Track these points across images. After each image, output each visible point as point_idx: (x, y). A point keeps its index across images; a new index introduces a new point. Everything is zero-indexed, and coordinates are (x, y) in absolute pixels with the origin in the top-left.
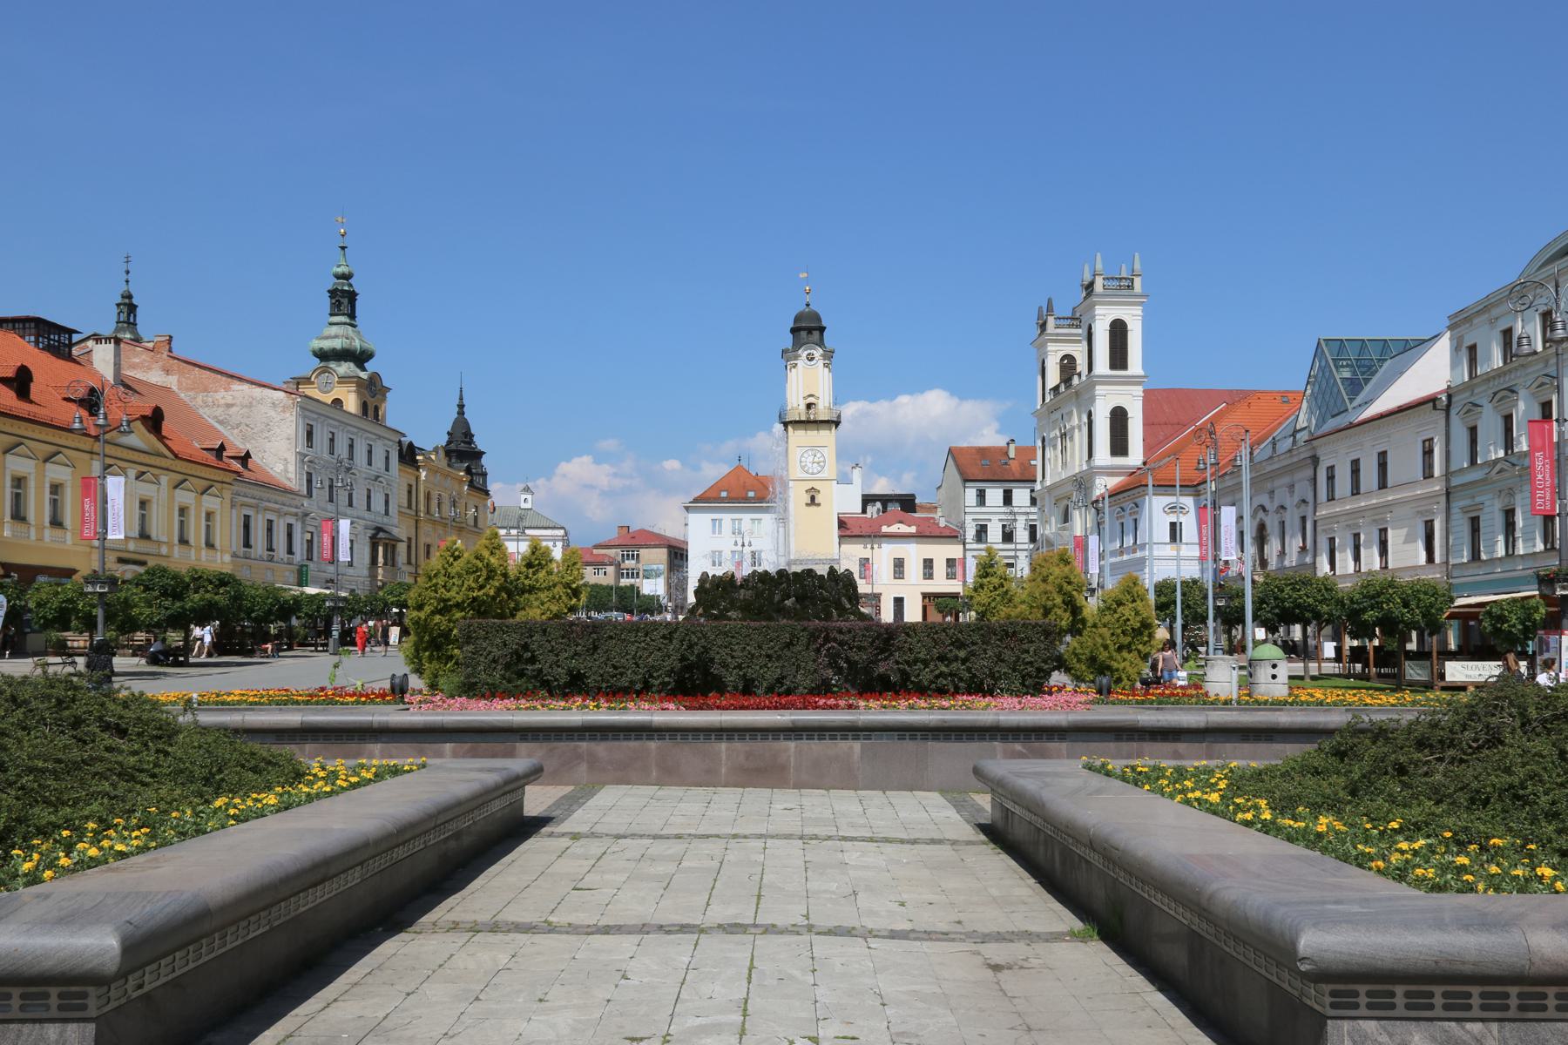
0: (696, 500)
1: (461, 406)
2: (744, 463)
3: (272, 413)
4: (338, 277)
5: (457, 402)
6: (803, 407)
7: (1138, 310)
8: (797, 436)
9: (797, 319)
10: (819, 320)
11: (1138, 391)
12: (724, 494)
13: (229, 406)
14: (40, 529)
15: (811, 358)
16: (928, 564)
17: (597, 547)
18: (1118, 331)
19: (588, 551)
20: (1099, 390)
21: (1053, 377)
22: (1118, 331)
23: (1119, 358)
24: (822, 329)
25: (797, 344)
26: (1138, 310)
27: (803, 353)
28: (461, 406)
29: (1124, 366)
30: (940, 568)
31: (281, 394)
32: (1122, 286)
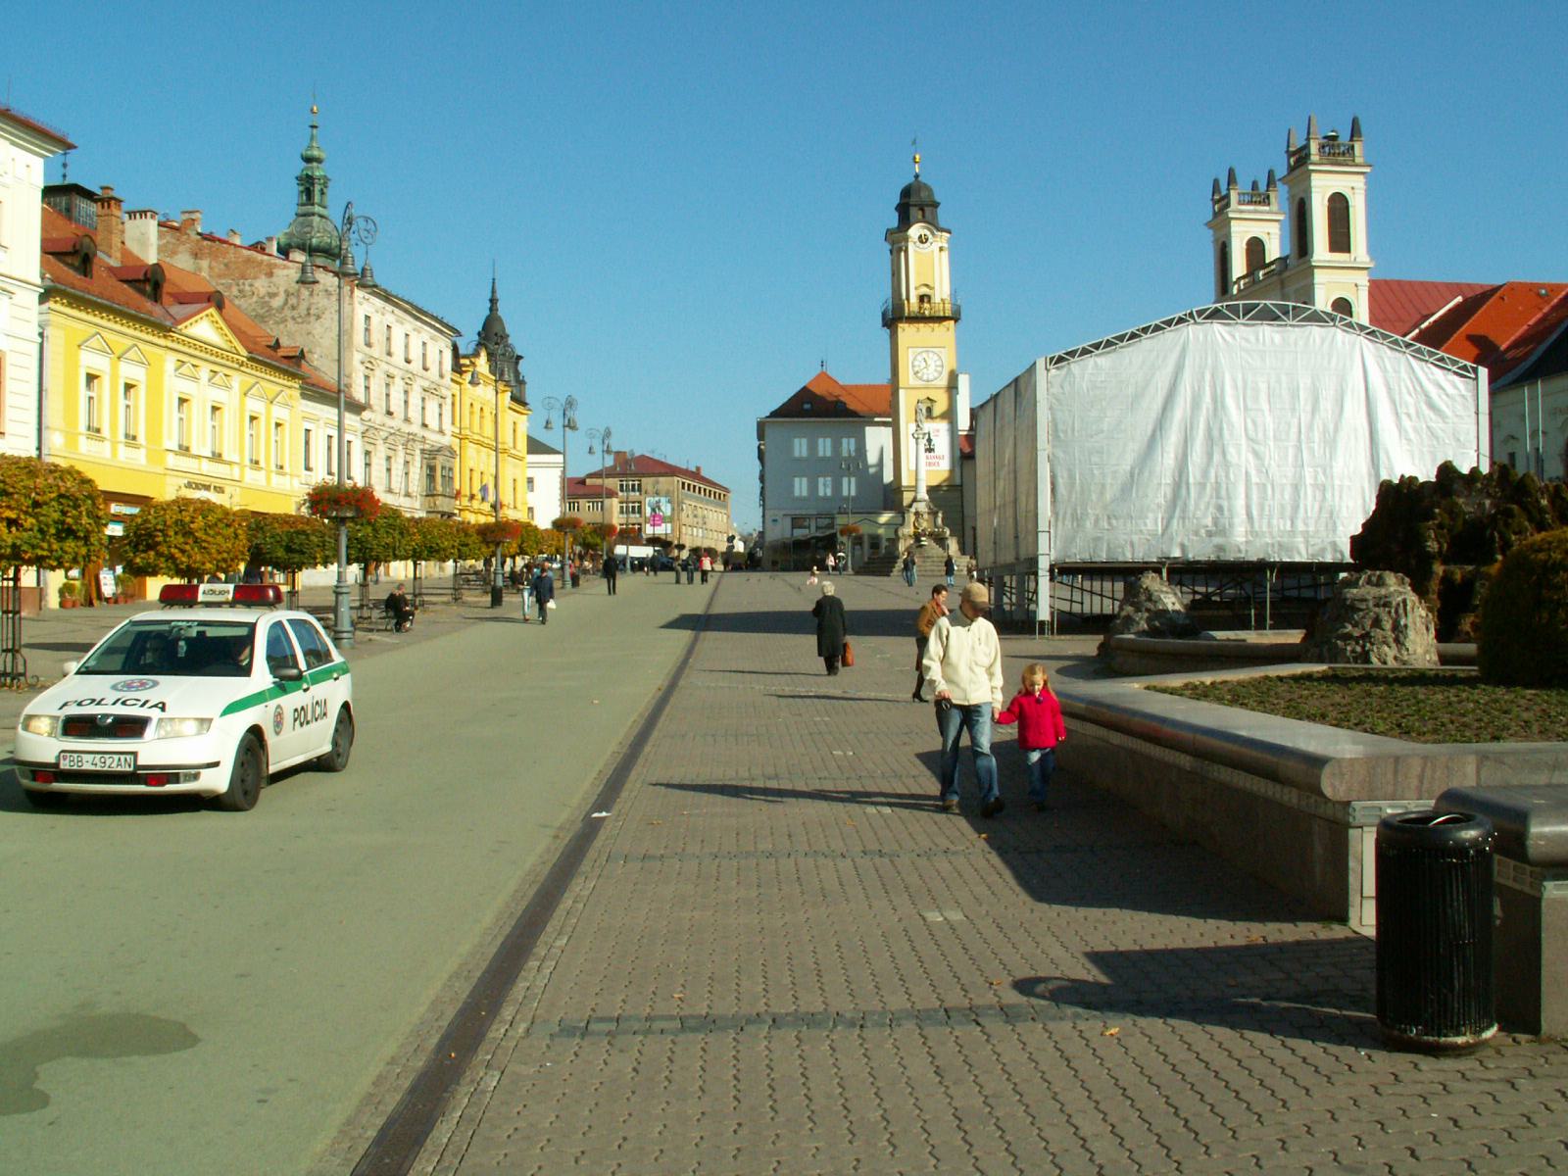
0: (775, 414)
1: (493, 301)
4: (308, 160)
5: (489, 296)
6: (914, 300)
7: (1359, 182)
8: (906, 332)
9: (906, 193)
11: (1363, 279)
12: (807, 406)
14: (114, 443)
15: (922, 240)
17: (591, 476)
18: (1339, 206)
19: (582, 482)
20: (1319, 277)
21: (1239, 267)
22: (1339, 206)
23: (1340, 240)
24: (935, 205)
25: (905, 222)
27: (915, 231)
28: (493, 301)
29: (1346, 249)
32: (1337, 151)
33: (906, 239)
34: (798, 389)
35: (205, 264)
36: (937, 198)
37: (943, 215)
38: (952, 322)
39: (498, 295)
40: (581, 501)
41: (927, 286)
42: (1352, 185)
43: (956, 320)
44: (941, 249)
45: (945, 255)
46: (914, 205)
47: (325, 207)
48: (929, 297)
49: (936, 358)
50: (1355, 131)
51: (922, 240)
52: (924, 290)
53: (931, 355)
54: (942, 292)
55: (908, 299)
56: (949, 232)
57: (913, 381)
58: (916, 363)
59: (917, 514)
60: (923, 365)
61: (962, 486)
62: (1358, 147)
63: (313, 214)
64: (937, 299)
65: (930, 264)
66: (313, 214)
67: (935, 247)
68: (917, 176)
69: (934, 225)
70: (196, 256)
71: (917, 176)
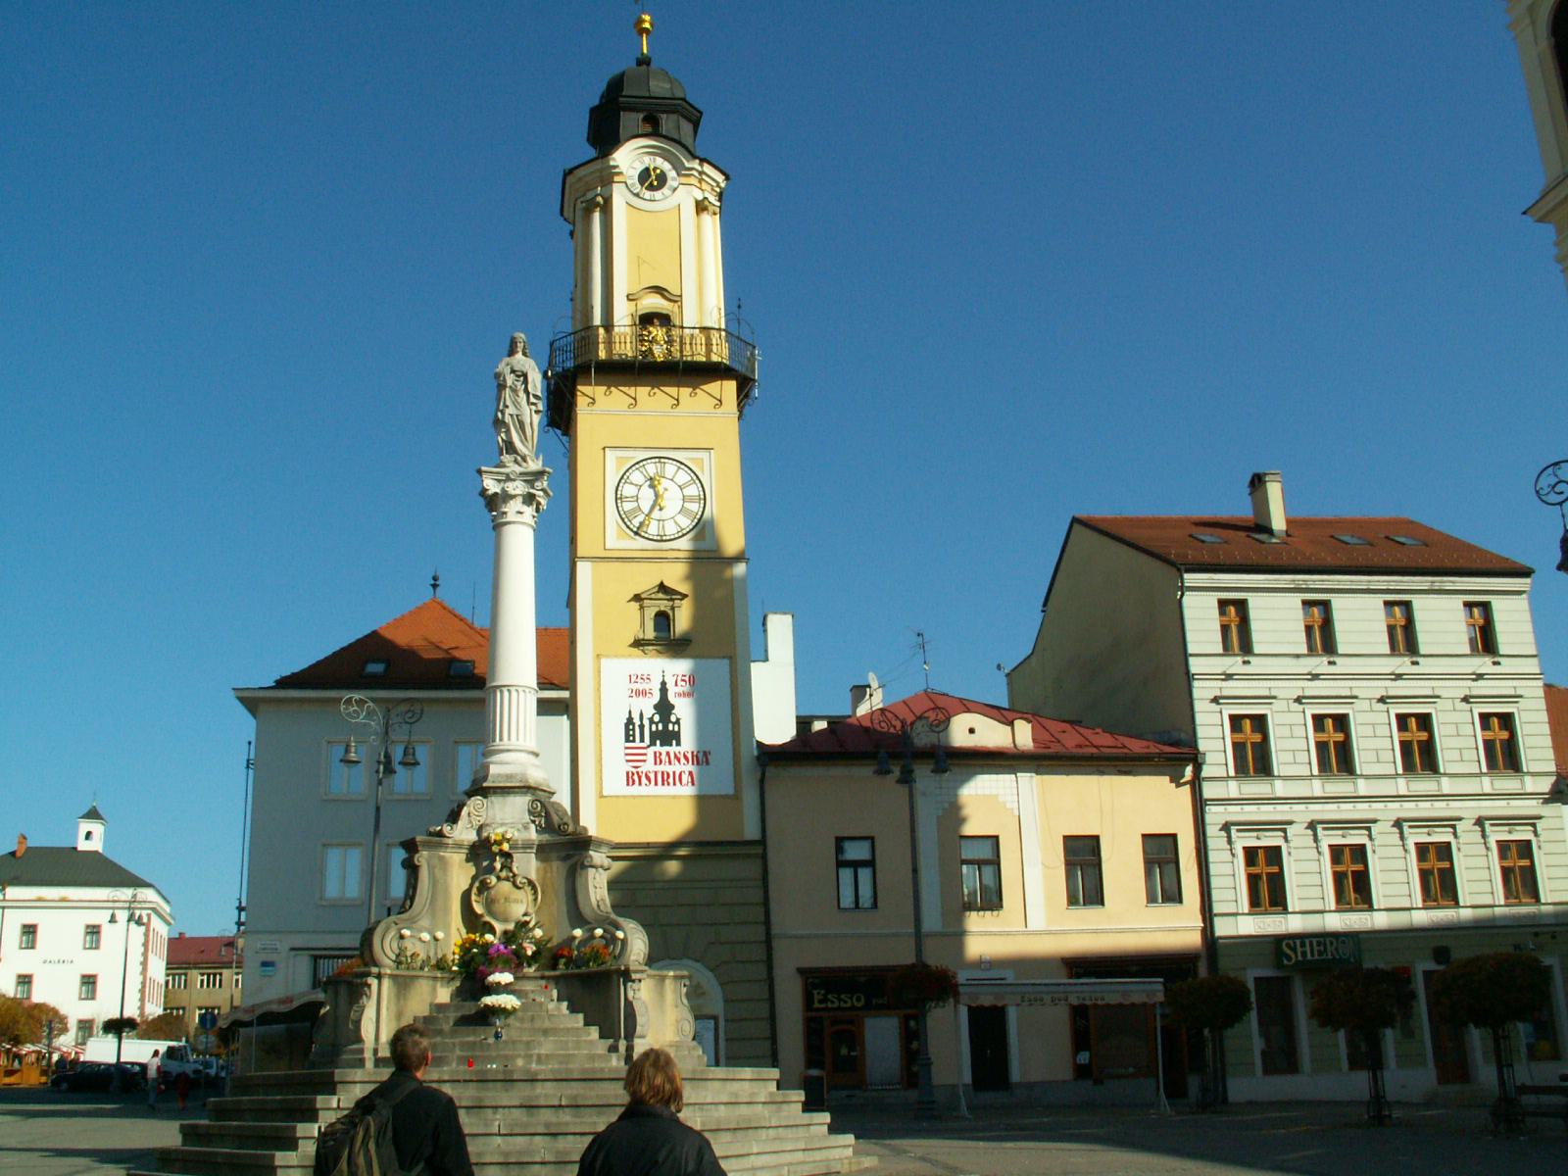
6: (623, 314)
15: (651, 180)
16: (1083, 857)
27: (630, 157)
30: (1123, 868)
33: (608, 177)
34: (367, 632)
38: (730, 387)
40: (226, 972)
41: (659, 290)
43: (745, 385)
44: (701, 207)
45: (711, 225)
48: (665, 320)
49: (683, 477)
51: (651, 180)
52: (653, 303)
53: (670, 469)
54: (703, 304)
55: (608, 326)
57: (617, 540)
58: (628, 490)
59: (482, 851)
60: (647, 495)
61: (762, 842)
71: (644, 61)
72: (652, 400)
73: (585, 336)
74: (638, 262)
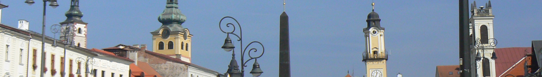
2: (350, 74)
3: (180, 71)
6: (372, 53)
7: (491, 21)
8: (370, 65)
9: (369, 16)
10: (378, 16)
13: (166, 69)
18: (484, 29)
22: (484, 29)
24: (380, 20)
25: (369, 27)
26: (491, 21)
27: (371, 30)
31: (183, 65)
33: (369, 32)
35: (147, 59)
36: (380, 18)
37: (382, 24)
38: (385, 60)
39: (235, 53)
42: (489, 23)
43: (387, 60)
44: (381, 35)
45: (382, 37)
46: (373, 21)
47: (177, 4)
50: (490, 6)
52: (375, 50)
56: (384, 29)
60: (375, 74)
62: (490, 10)
63: (173, 7)
64: (379, 53)
65: (377, 41)
66: (173, 7)
67: (379, 35)
68: (373, 10)
69: (379, 28)
70: (145, 57)
72: (375, 63)
73: (367, 55)
74: (373, 44)
